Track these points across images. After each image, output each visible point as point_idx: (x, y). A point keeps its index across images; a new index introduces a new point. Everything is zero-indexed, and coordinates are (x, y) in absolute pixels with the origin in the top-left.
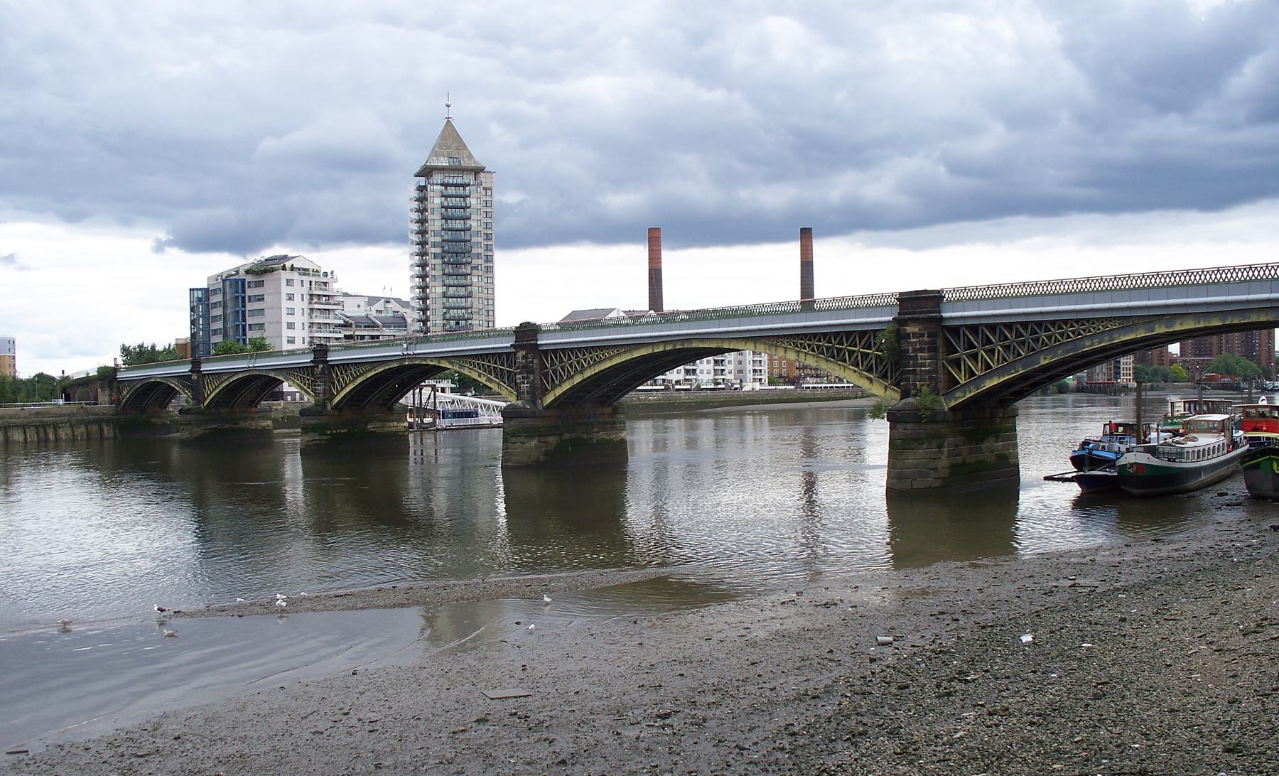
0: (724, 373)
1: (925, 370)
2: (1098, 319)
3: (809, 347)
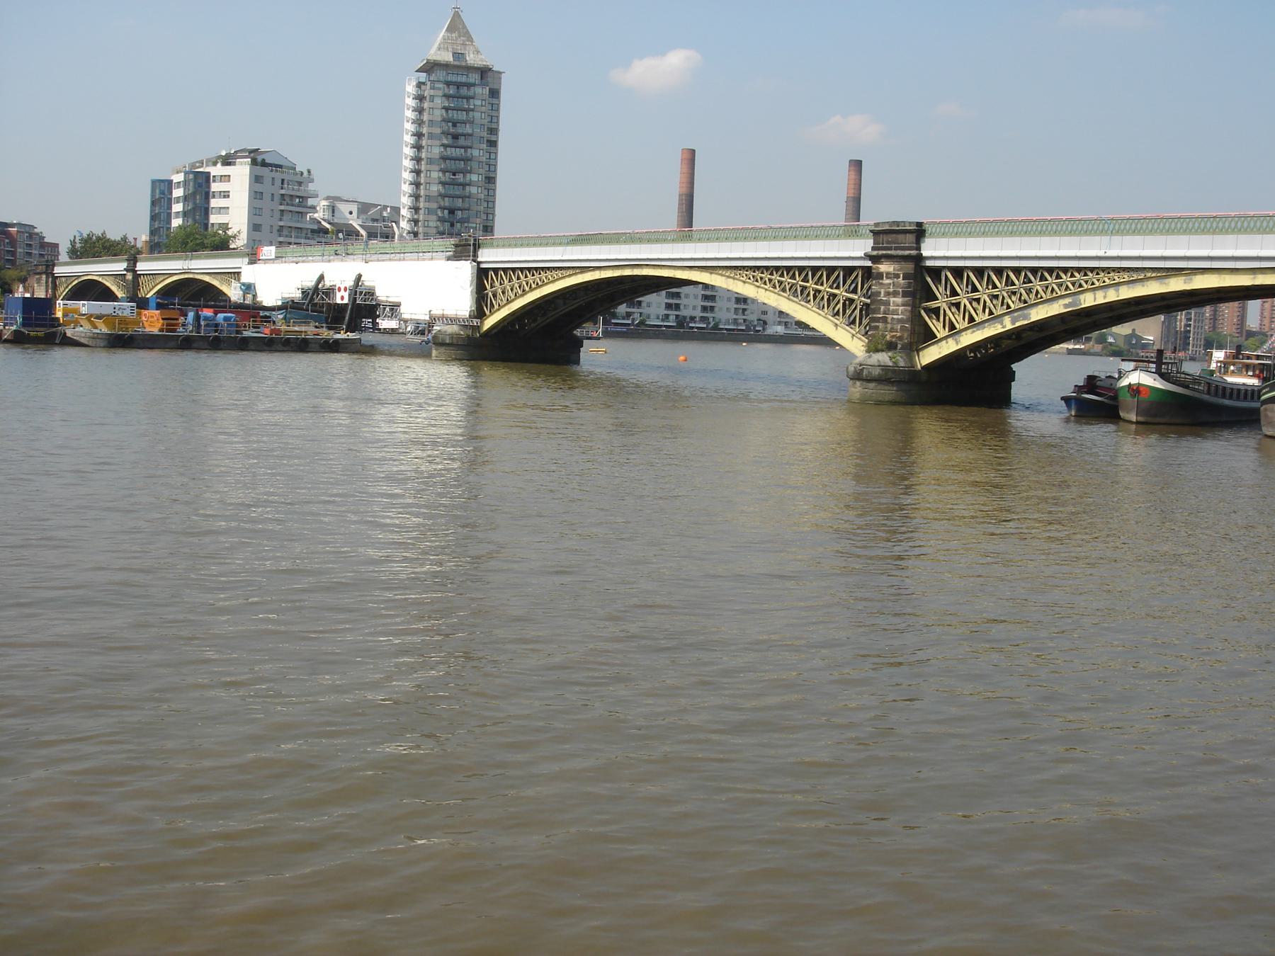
0: (746, 313)
1: (898, 319)
2: (1103, 269)
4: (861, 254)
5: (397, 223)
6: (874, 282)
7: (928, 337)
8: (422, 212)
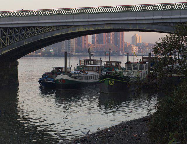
2: (47, 27)
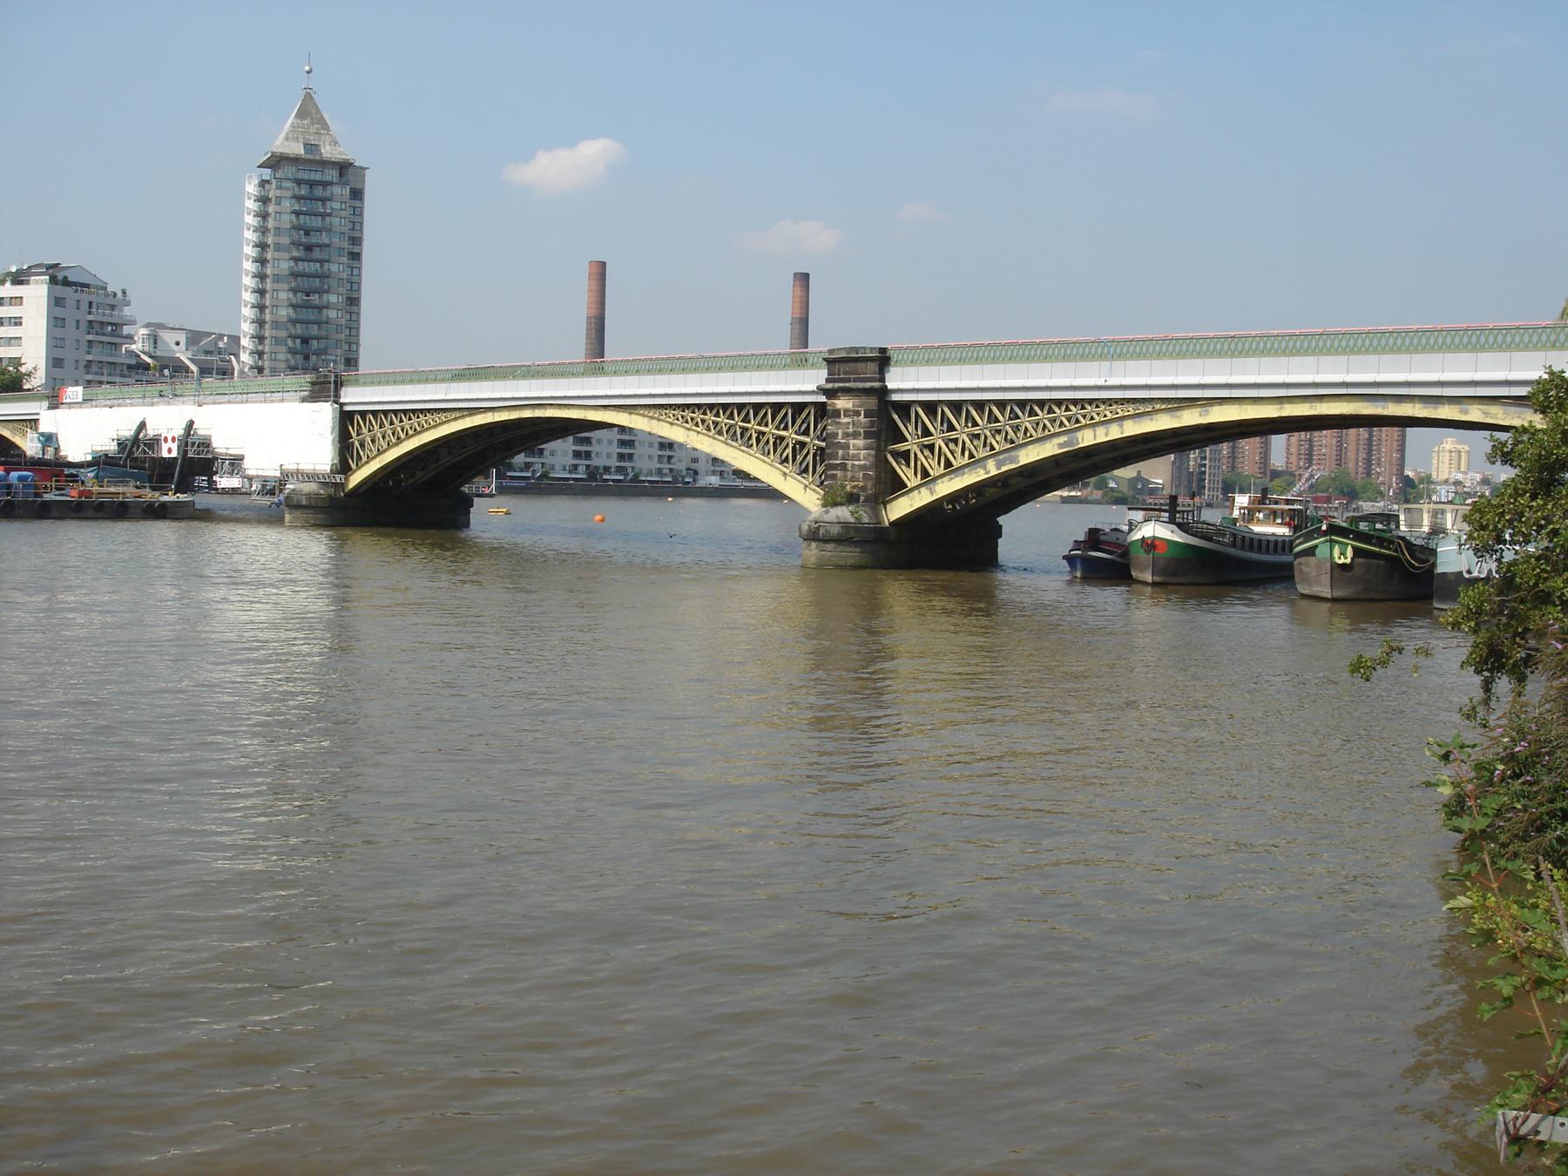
0: (672, 461)
1: (859, 466)
2: (1104, 401)
3: (703, 424)
4: (813, 387)
5: (237, 356)
6: (830, 421)
7: (897, 487)
8: (267, 342)
